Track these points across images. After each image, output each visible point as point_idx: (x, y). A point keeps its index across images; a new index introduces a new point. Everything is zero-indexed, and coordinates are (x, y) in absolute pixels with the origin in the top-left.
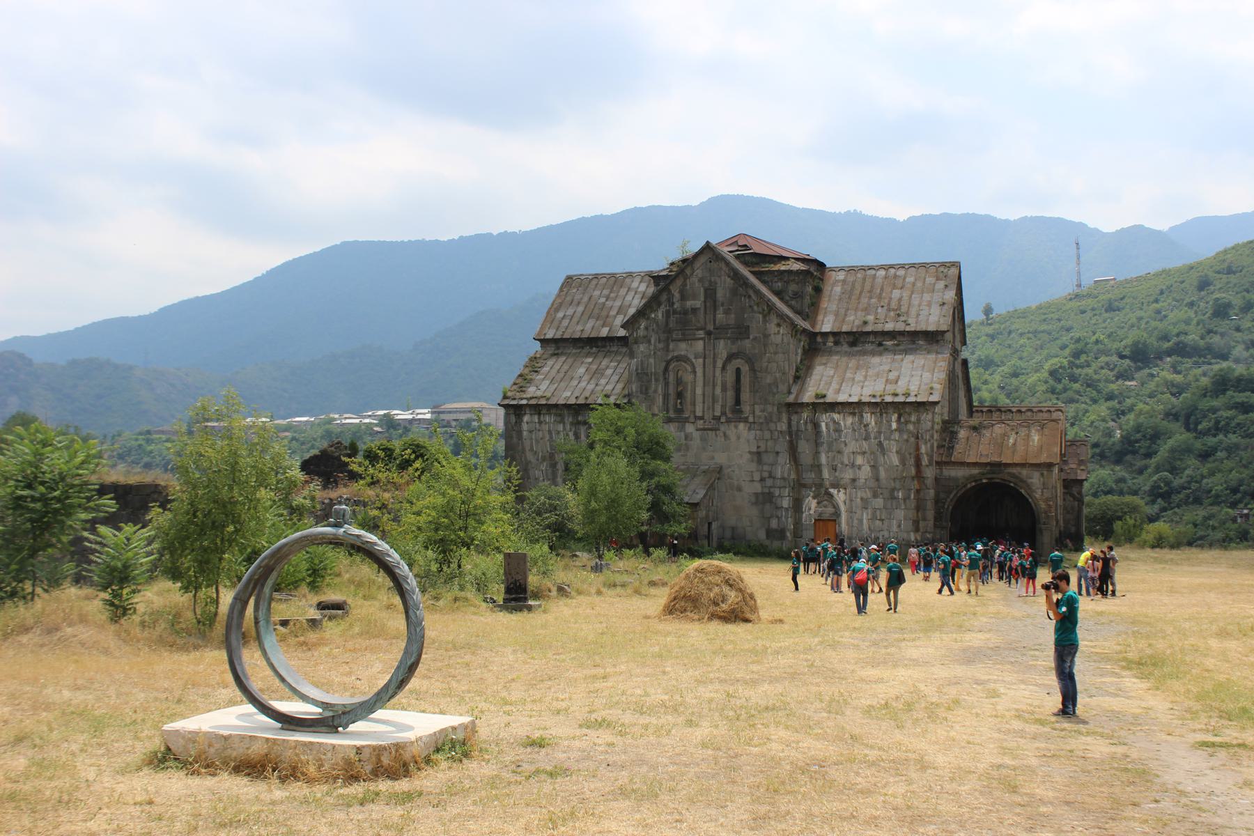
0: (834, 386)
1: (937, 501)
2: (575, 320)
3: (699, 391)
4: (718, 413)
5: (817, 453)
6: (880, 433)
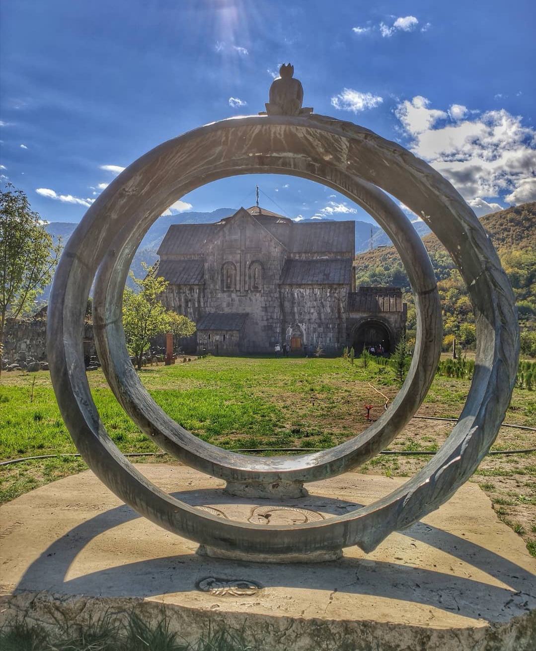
1: (347, 329)
3: (238, 278)
5: (293, 307)
6: (322, 298)
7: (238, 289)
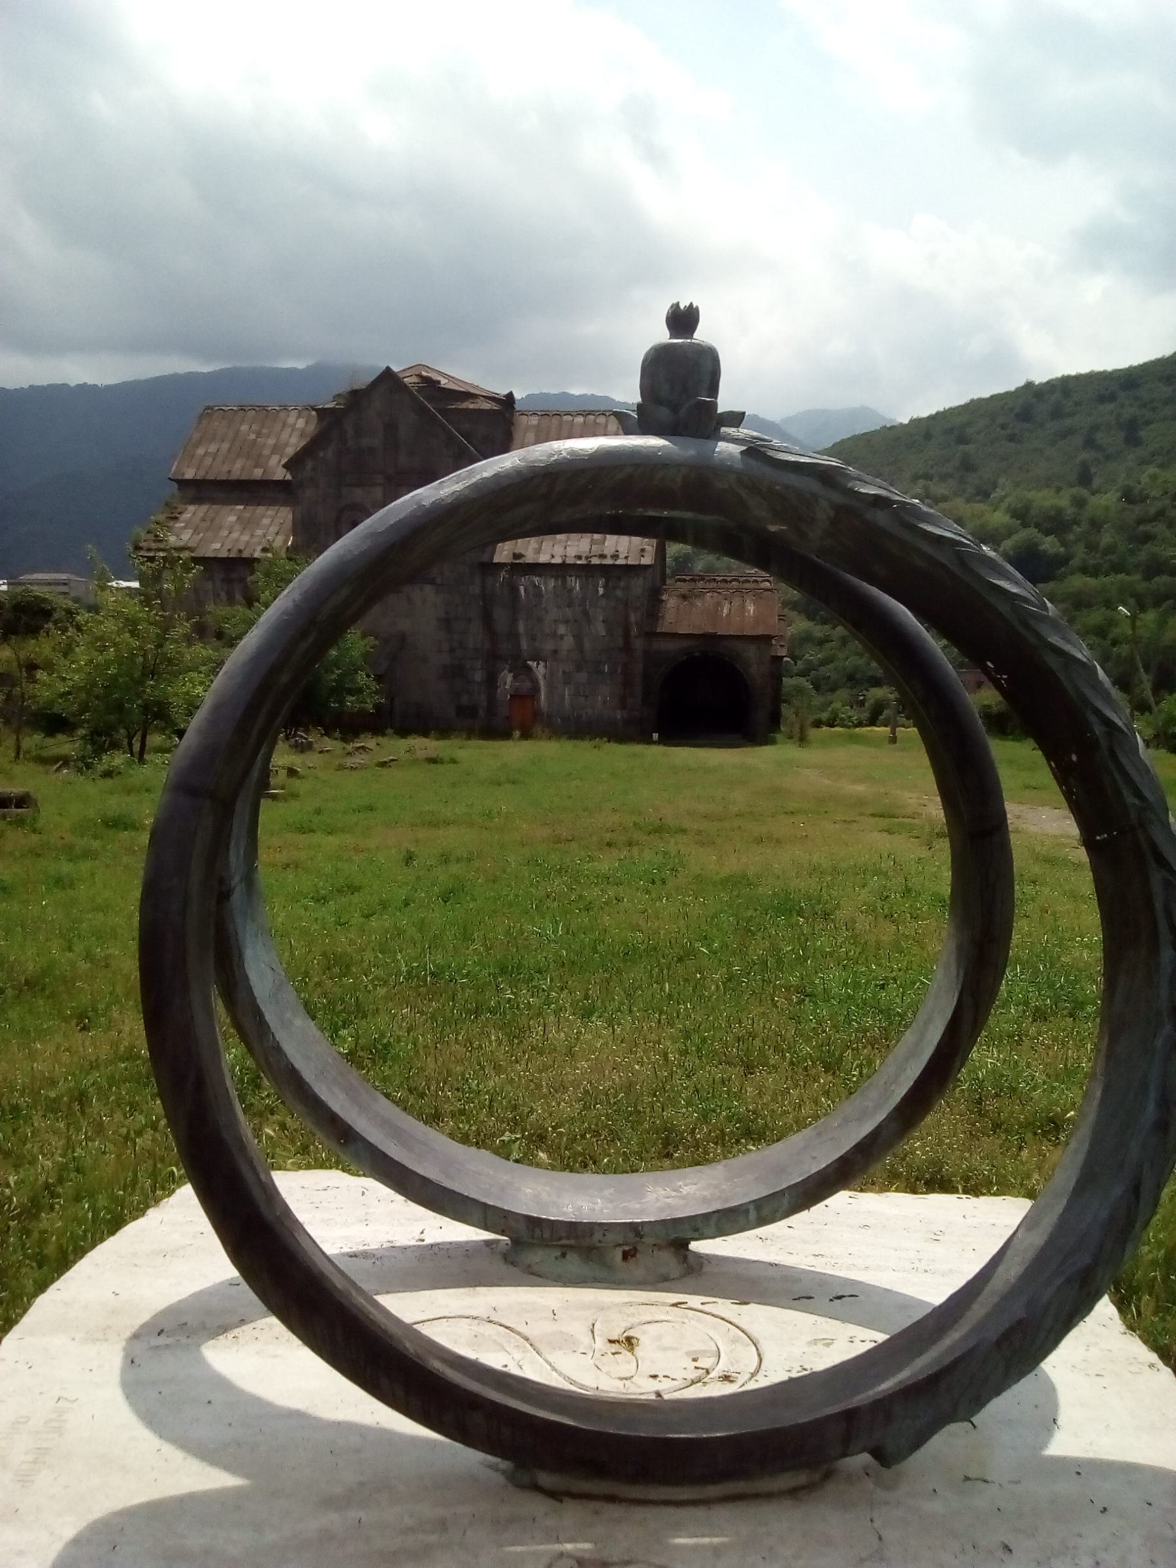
5: (514, 622)
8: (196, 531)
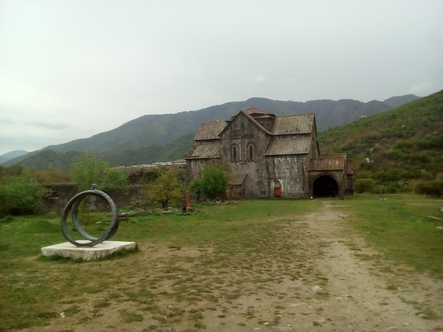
0: (279, 150)
1: (309, 182)
2: (205, 134)
3: (240, 153)
4: (246, 159)
5: (274, 169)
6: (292, 163)
7: (240, 159)
8: (199, 152)
